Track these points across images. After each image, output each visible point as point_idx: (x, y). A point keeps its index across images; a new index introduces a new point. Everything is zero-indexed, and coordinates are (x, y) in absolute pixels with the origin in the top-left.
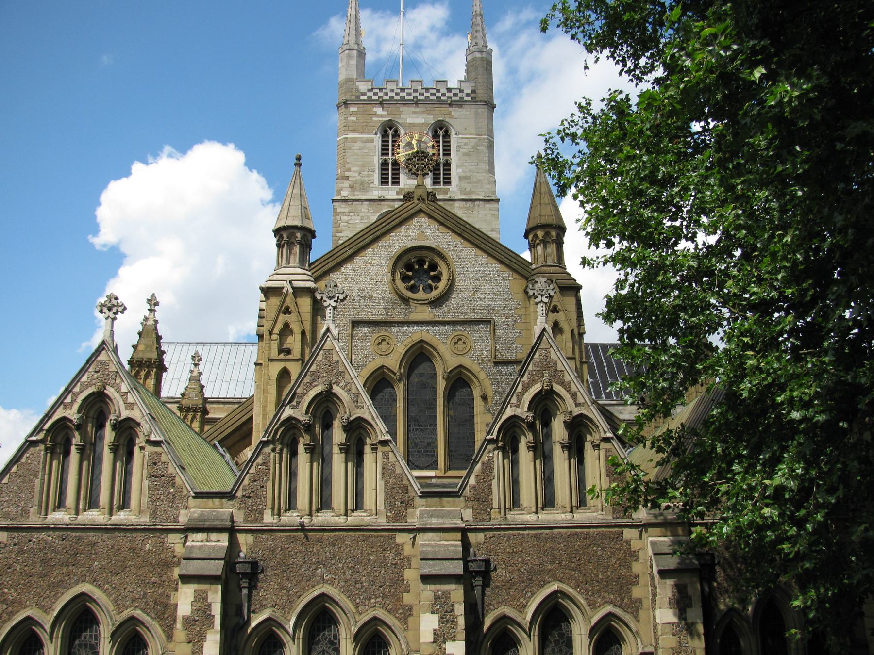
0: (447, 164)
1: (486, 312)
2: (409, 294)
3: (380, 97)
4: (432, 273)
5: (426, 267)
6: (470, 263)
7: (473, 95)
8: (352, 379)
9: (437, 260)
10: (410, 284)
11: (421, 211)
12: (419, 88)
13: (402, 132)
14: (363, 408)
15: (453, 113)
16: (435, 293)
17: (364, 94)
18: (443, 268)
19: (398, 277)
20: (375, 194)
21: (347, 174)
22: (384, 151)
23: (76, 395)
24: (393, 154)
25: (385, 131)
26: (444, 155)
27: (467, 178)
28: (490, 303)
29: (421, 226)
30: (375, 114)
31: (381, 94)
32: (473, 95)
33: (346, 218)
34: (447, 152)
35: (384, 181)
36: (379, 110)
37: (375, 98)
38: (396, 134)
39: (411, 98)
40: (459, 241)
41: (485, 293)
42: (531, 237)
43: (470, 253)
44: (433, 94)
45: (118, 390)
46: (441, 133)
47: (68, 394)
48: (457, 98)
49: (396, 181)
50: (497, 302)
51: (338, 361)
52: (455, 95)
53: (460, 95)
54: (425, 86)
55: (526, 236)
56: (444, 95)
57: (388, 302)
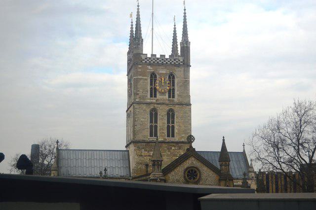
0: (174, 90)
3: (150, 62)
9: (196, 169)
11: (192, 155)
13: (158, 76)
16: (196, 180)
20: (148, 101)
21: (138, 92)
22: (151, 84)
24: (154, 85)
25: (151, 75)
27: (180, 96)
30: (148, 69)
31: (150, 60)
33: (138, 110)
34: (173, 85)
35: (151, 96)
36: (149, 67)
37: (148, 62)
38: (156, 76)
39: (161, 62)
40: (202, 165)
43: (205, 168)
44: (169, 61)
46: (171, 77)
49: (155, 96)
52: (177, 62)
54: (166, 58)
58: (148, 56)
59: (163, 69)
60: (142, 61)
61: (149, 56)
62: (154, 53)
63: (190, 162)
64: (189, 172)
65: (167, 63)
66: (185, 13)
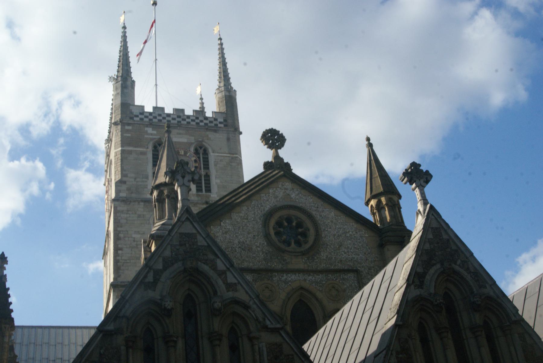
0: (207, 176)
1: (351, 264)
2: (283, 246)
3: (150, 120)
4: (300, 230)
5: (294, 224)
6: (332, 222)
7: (225, 123)
8: (467, 258)
9: (303, 217)
10: (283, 238)
12: (181, 114)
14: (485, 287)
15: (210, 136)
17: (137, 116)
18: (308, 224)
19: (272, 232)
23: (158, 274)
26: (204, 168)
28: (354, 256)
29: (286, 189)
30: (146, 132)
32: (225, 123)
33: (126, 216)
36: (150, 130)
41: (348, 248)
42: (373, 202)
44: (193, 120)
45: (214, 268)
46: (201, 151)
47: (148, 272)
48: (213, 125)
50: (359, 255)
51: (448, 240)
52: (211, 122)
53: (215, 122)
55: (367, 204)
56: (202, 121)
57: (266, 253)
58: (146, 110)
59: (178, 134)
60: (132, 118)
61: (149, 109)
62: (159, 106)
63: (280, 194)
64: (279, 224)
65: (189, 123)
66: (221, 44)
